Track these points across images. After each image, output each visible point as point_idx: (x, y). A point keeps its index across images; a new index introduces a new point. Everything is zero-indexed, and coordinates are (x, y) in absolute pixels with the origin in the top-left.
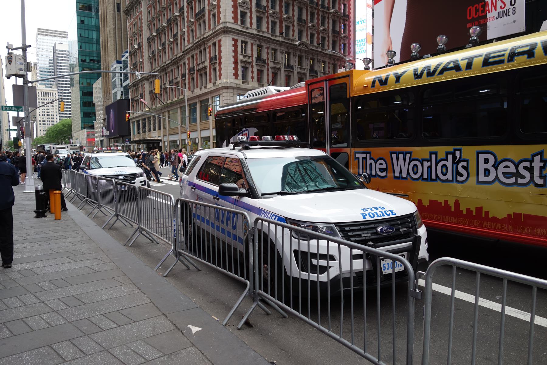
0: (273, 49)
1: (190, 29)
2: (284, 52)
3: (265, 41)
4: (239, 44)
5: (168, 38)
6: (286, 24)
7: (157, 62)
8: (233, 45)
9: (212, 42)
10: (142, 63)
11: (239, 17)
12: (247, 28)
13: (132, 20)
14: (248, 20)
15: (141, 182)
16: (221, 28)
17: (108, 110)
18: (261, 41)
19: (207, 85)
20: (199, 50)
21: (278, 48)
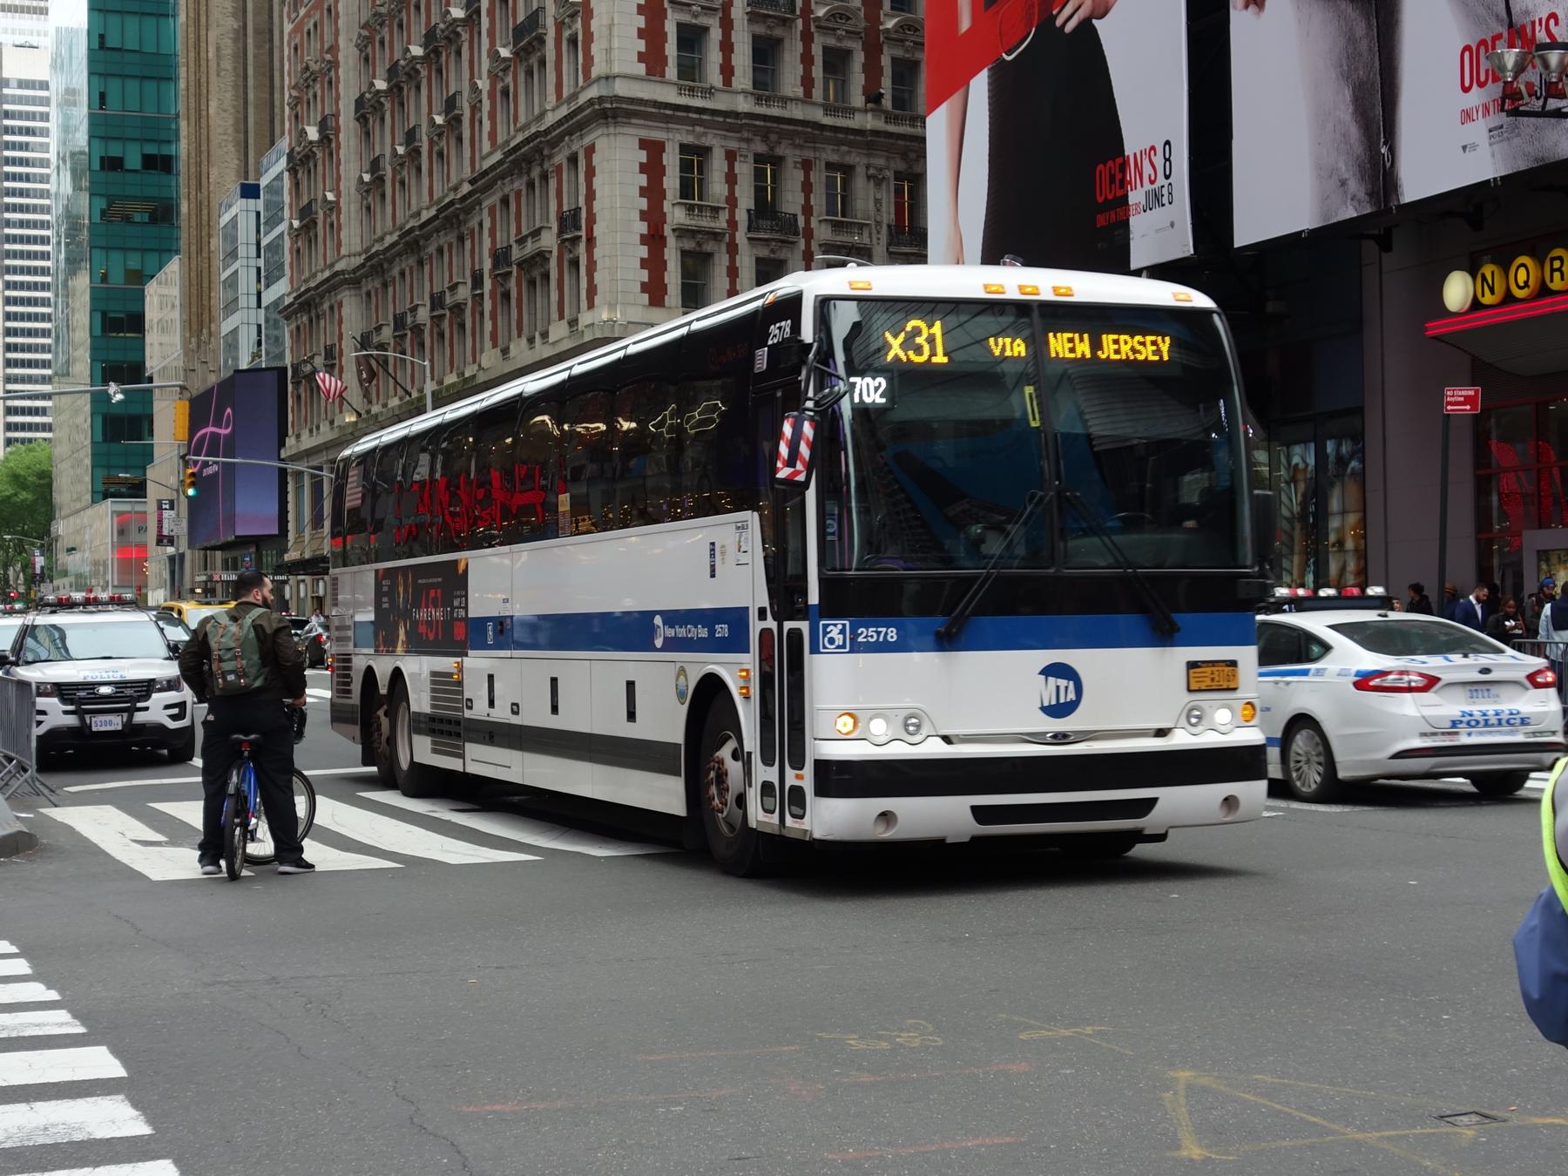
0: (830, 166)
1: (499, 86)
2: (889, 174)
3: (791, 135)
4: (671, 160)
5: (426, 113)
6: (899, 53)
7: (389, 209)
8: (643, 168)
9: (567, 153)
10: (334, 207)
11: (671, 49)
12: (709, 92)
13: (302, 11)
14: (714, 57)
15: (167, 707)
16: (591, 102)
17: (200, 409)
18: (773, 137)
19: (551, 329)
20: (525, 178)
21: (856, 159)
